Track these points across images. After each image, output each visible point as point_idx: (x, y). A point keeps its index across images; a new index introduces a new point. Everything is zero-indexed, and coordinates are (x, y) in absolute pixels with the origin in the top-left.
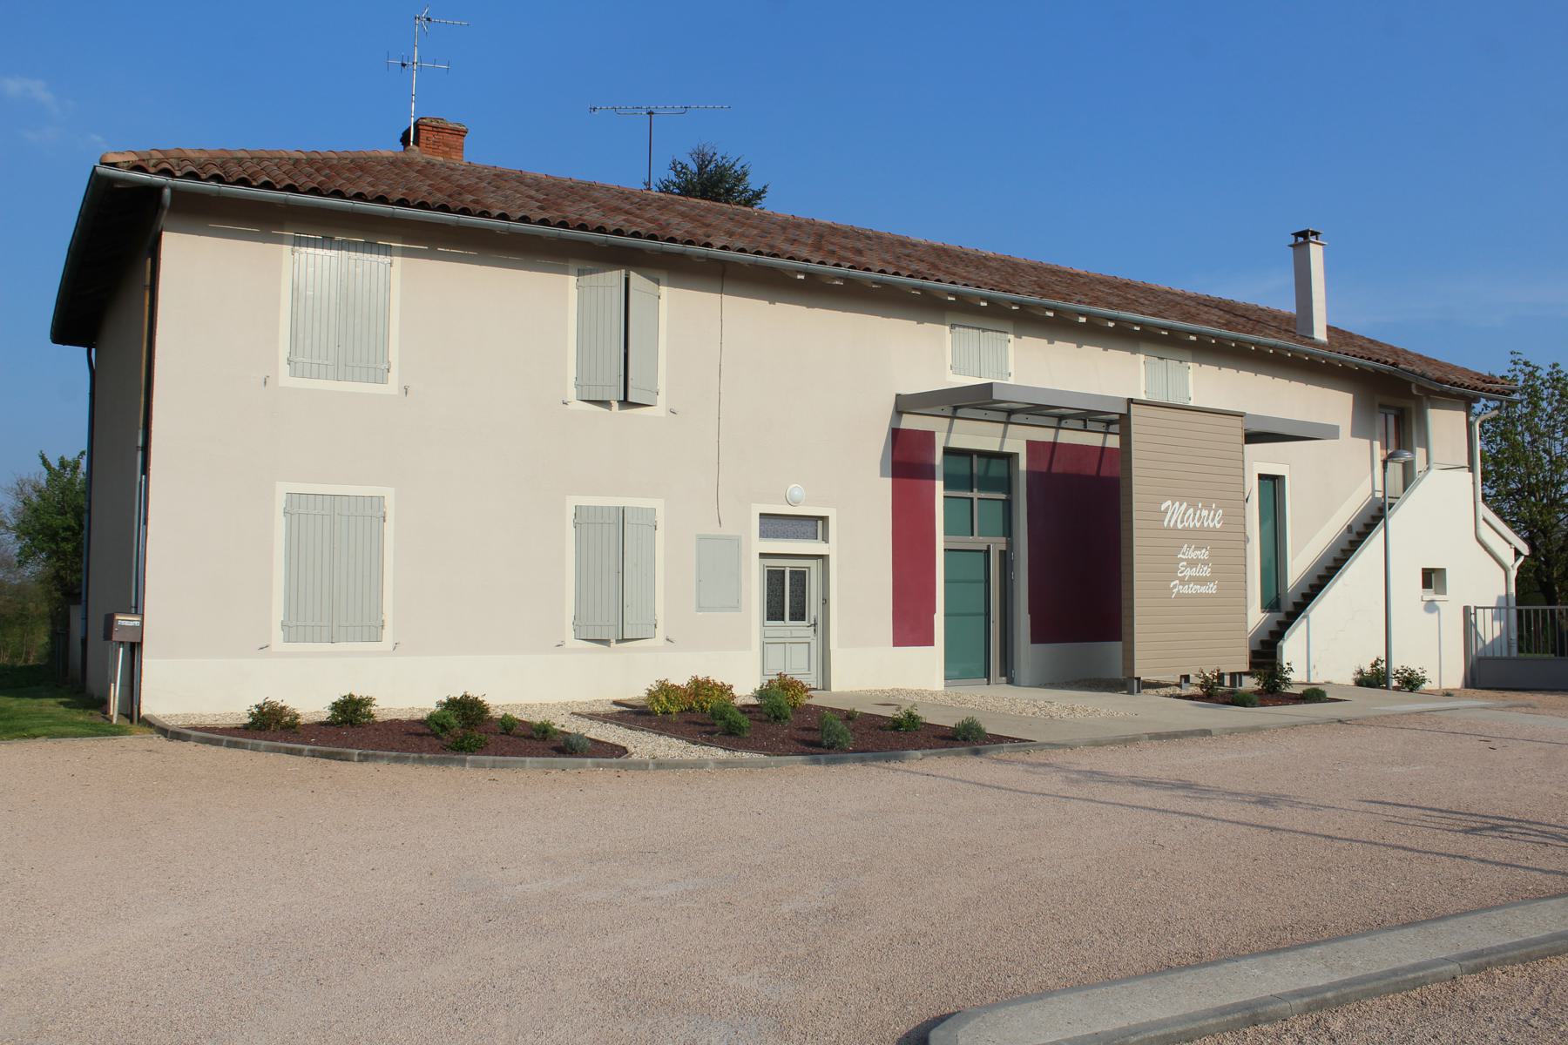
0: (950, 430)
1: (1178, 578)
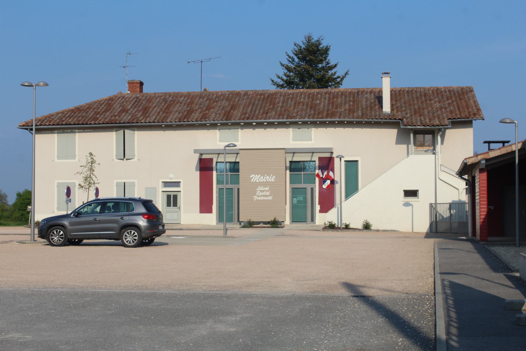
1: (257, 195)
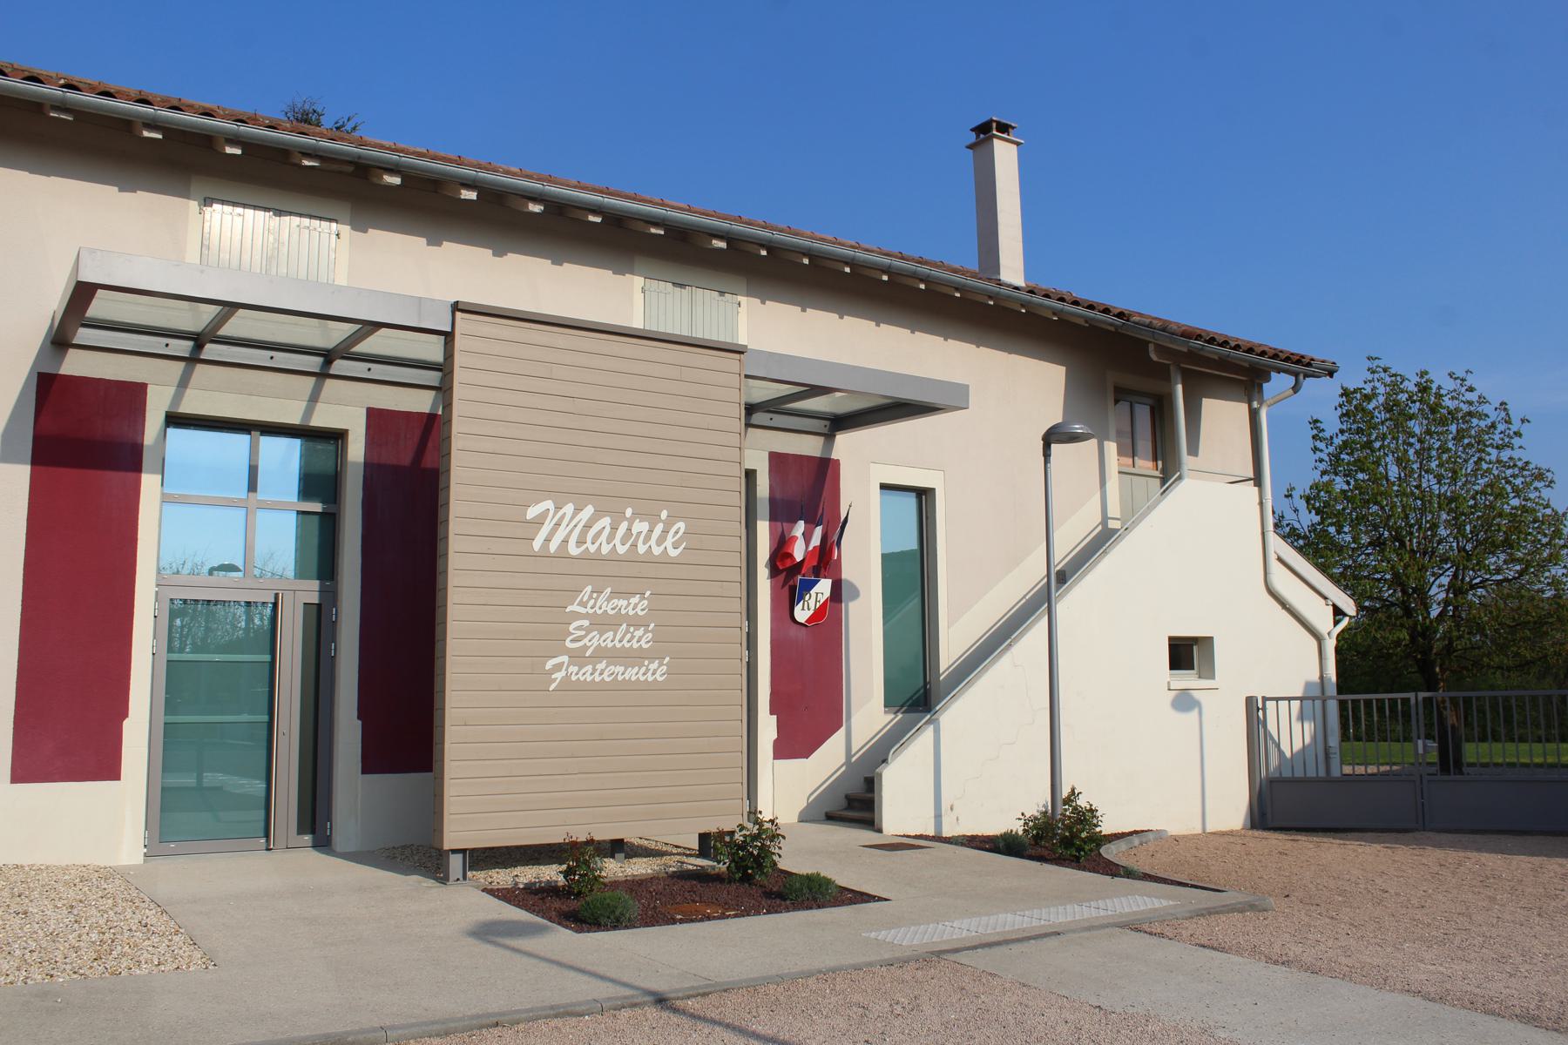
0: (183, 383)
1: (567, 651)
